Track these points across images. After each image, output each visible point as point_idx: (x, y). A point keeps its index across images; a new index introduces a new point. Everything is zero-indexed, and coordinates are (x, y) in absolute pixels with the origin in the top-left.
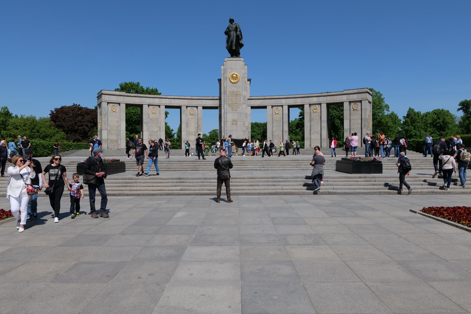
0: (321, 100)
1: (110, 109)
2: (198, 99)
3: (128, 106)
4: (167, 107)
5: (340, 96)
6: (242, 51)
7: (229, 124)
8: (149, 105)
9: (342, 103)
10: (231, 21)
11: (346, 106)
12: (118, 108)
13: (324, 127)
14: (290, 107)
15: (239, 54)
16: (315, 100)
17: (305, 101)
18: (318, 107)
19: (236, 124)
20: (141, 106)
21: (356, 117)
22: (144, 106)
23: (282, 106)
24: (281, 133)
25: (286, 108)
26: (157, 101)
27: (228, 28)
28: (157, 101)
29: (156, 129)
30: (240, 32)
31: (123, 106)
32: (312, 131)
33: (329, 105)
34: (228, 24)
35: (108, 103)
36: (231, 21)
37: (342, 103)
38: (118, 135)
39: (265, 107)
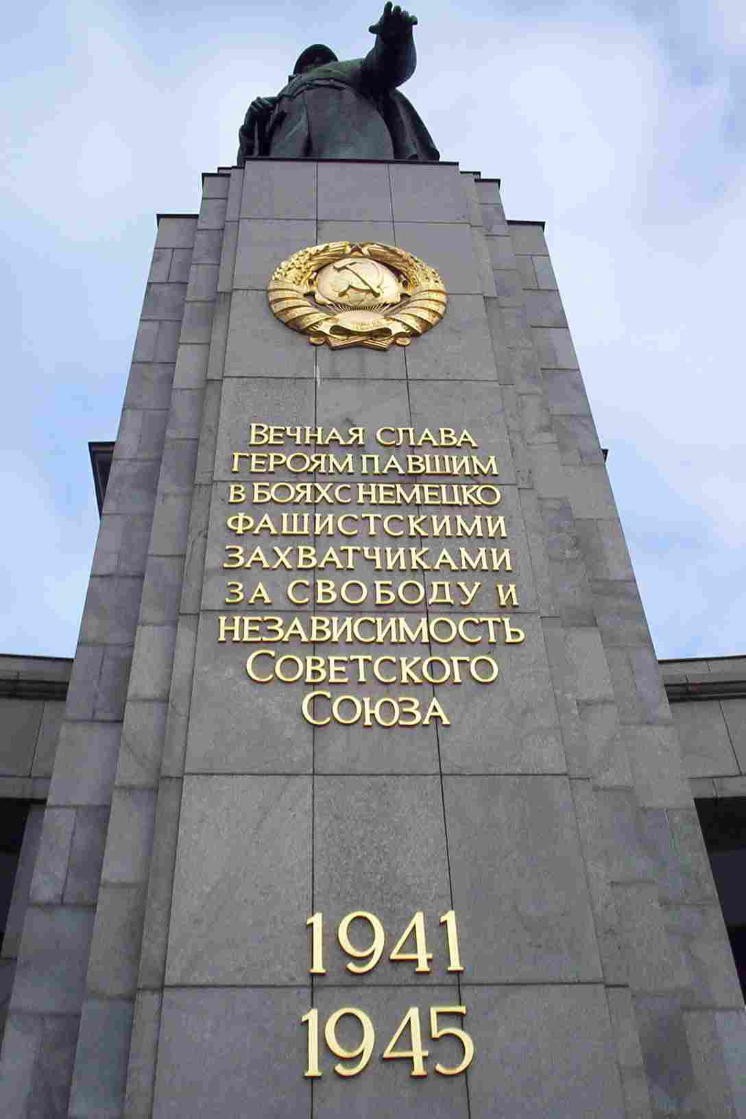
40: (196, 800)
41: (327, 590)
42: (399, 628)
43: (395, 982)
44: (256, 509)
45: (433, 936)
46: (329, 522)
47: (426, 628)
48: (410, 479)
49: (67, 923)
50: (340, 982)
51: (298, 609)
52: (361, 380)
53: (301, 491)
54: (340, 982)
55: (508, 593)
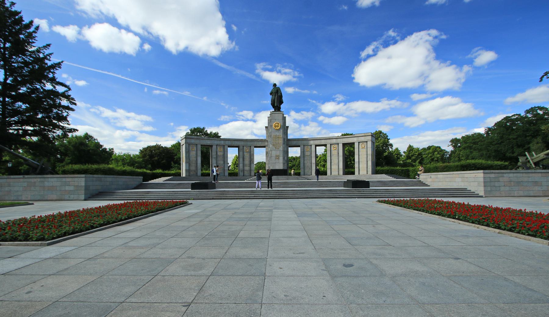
0: (339, 141)
3: (201, 145)
9: (354, 143)
11: (356, 145)
16: (334, 141)
17: (328, 142)
18: (336, 146)
19: (278, 158)
20: (211, 146)
25: (313, 147)
27: (272, 91)
28: (222, 142)
29: (222, 162)
33: (344, 145)
37: (354, 143)
39: (299, 146)
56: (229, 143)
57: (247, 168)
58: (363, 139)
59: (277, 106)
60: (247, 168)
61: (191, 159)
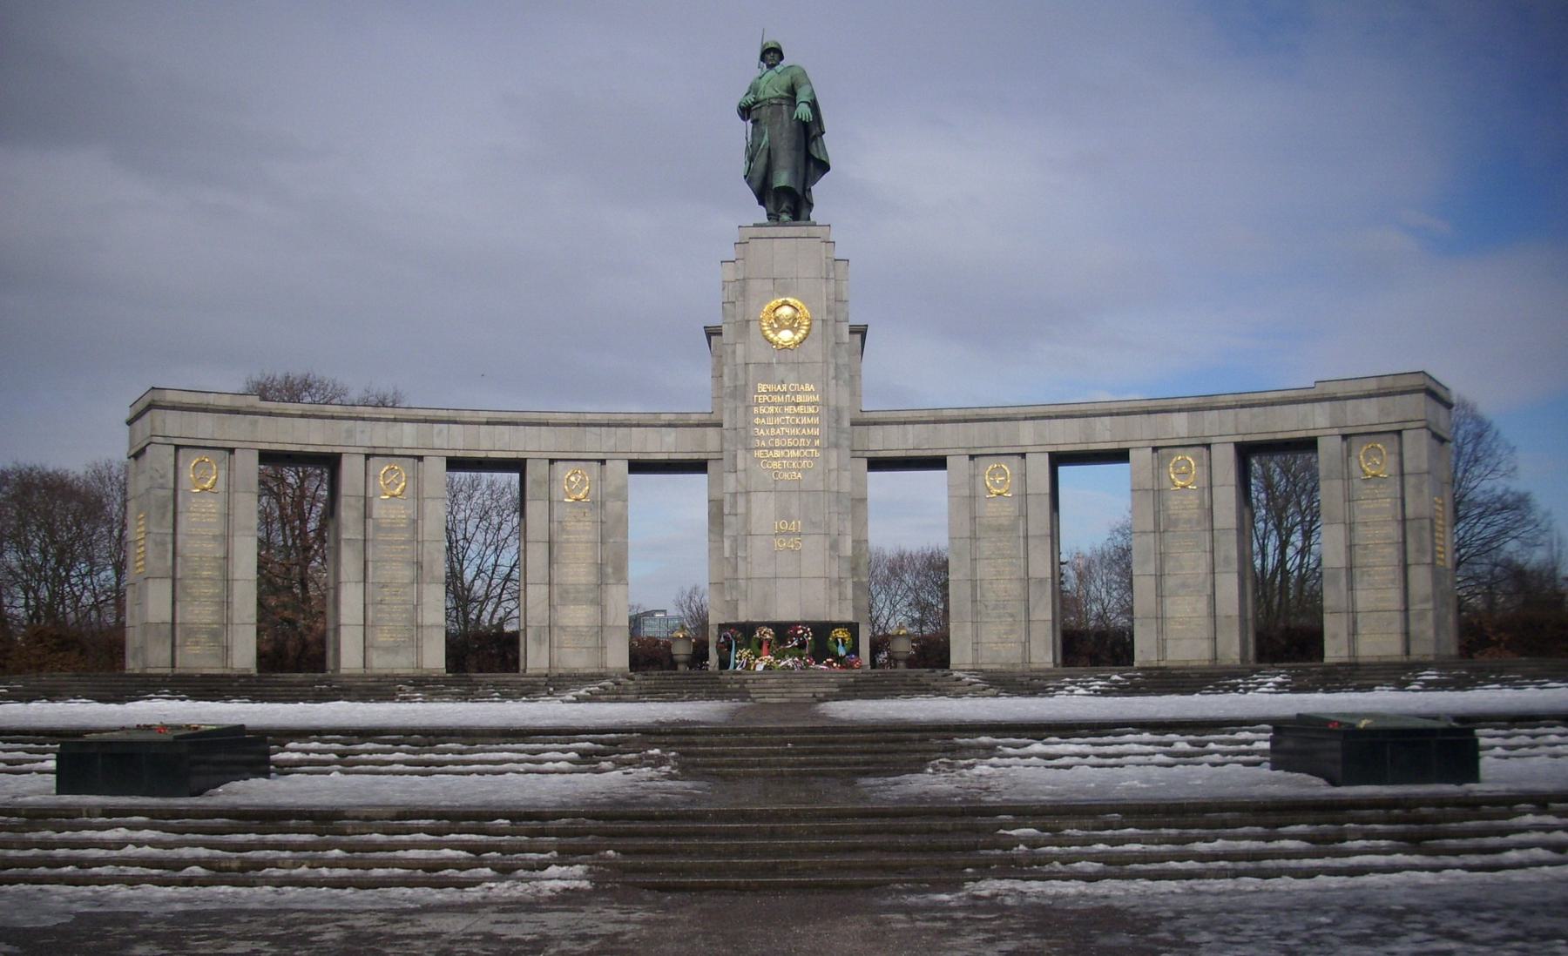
0: (1210, 424)
1: (188, 474)
2: (608, 425)
3: (266, 457)
4: (454, 464)
5: (1301, 406)
6: (819, 190)
7: (758, 544)
8: (367, 456)
9: (1310, 444)
10: (772, 55)
12: (223, 473)
13: (1227, 560)
14: (1058, 460)
15: (810, 205)
16: (1179, 425)
20: (330, 462)
21: (1377, 508)
22: (345, 461)
23: (1023, 455)
24: (1016, 589)
25: (1039, 466)
26: (407, 436)
27: (754, 89)
28: (407, 436)
29: (405, 574)
30: (814, 106)
31: (248, 465)
32: (1170, 582)
34: (752, 67)
35: (177, 447)
36: (772, 55)
38: (225, 603)
39: (938, 463)
40: (753, 496)
41: (778, 443)
42: (792, 453)
43: (788, 534)
44: (761, 416)
45: (796, 525)
46: (778, 420)
47: (798, 454)
48: (797, 405)
49: (733, 519)
50: (780, 534)
51: (770, 449)
52: (786, 364)
53: (771, 409)
54: (780, 534)
55: (817, 443)
56: (460, 441)
57: (577, 616)
58: (1369, 413)
59: (786, 191)
60: (577, 616)
61: (187, 546)
